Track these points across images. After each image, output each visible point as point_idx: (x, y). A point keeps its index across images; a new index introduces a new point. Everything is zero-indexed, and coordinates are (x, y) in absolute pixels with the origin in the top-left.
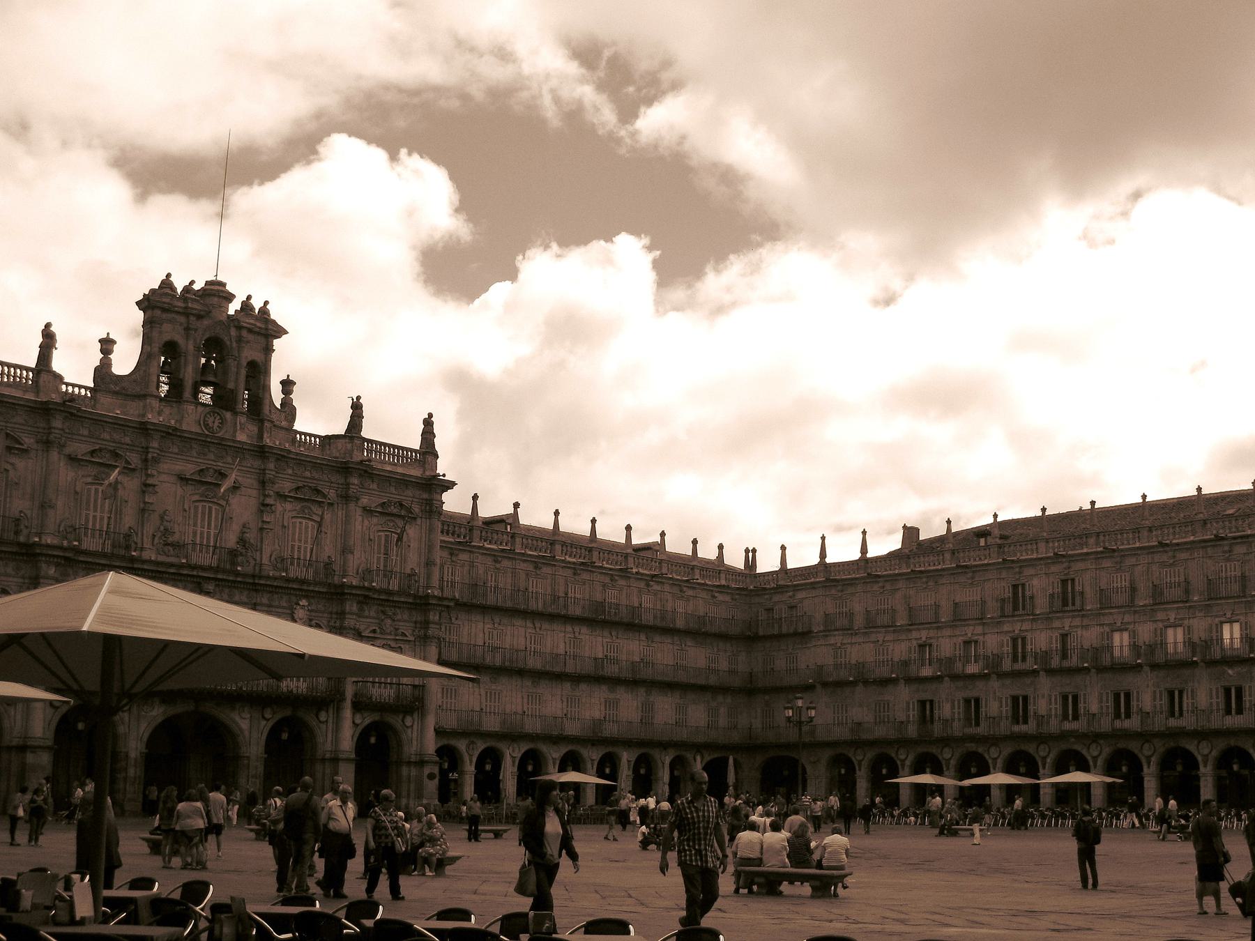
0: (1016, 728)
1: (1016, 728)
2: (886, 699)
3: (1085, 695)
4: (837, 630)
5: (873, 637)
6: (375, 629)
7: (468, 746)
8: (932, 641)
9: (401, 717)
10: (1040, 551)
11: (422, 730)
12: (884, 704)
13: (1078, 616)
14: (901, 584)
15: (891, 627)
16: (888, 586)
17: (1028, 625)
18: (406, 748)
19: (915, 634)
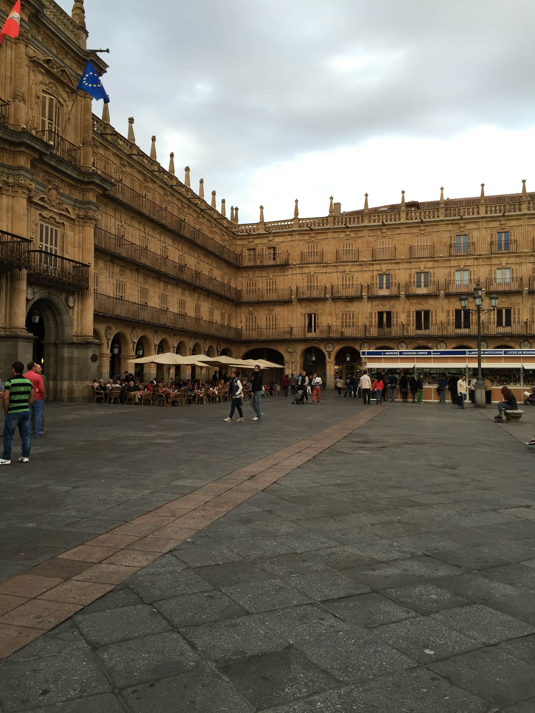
0: (458, 331)
1: (458, 331)
2: (352, 310)
3: (519, 309)
4: (311, 263)
5: (341, 269)
6: (44, 198)
7: (106, 331)
8: (390, 272)
9: (64, 296)
10: (481, 212)
11: (82, 311)
12: (350, 314)
13: (514, 256)
14: (366, 233)
15: (356, 262)
16: (353, 235)
17: (471, 262)
18: (67, 330)
19: (376, 267)
